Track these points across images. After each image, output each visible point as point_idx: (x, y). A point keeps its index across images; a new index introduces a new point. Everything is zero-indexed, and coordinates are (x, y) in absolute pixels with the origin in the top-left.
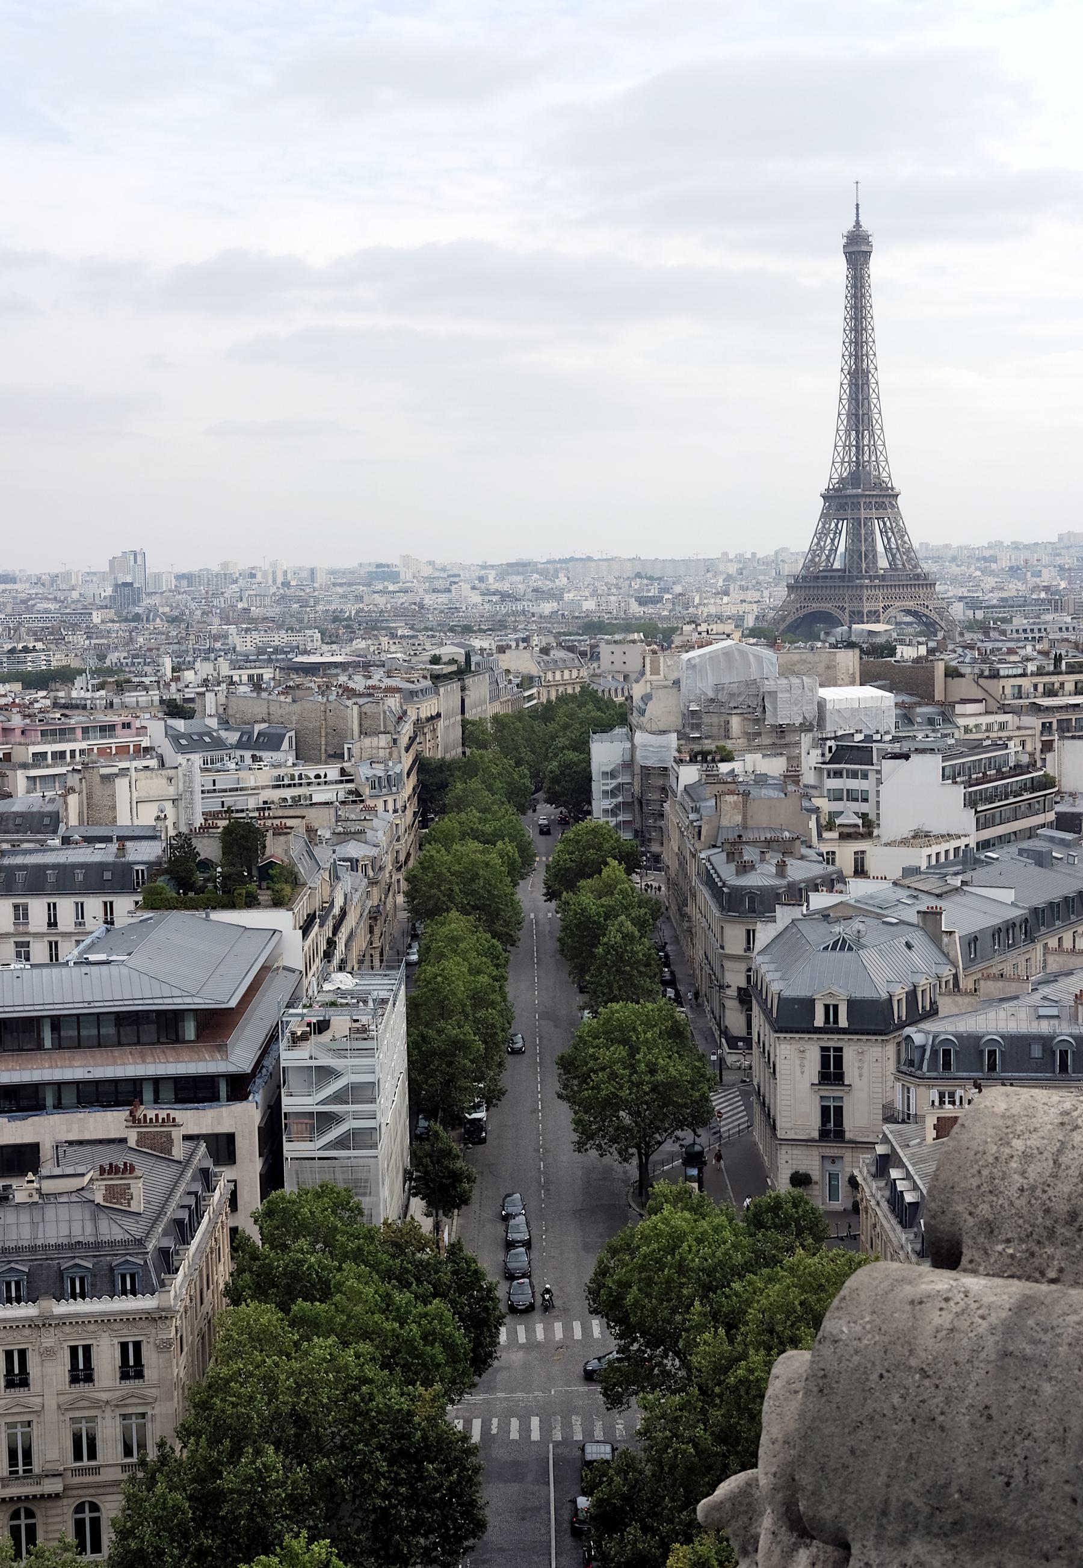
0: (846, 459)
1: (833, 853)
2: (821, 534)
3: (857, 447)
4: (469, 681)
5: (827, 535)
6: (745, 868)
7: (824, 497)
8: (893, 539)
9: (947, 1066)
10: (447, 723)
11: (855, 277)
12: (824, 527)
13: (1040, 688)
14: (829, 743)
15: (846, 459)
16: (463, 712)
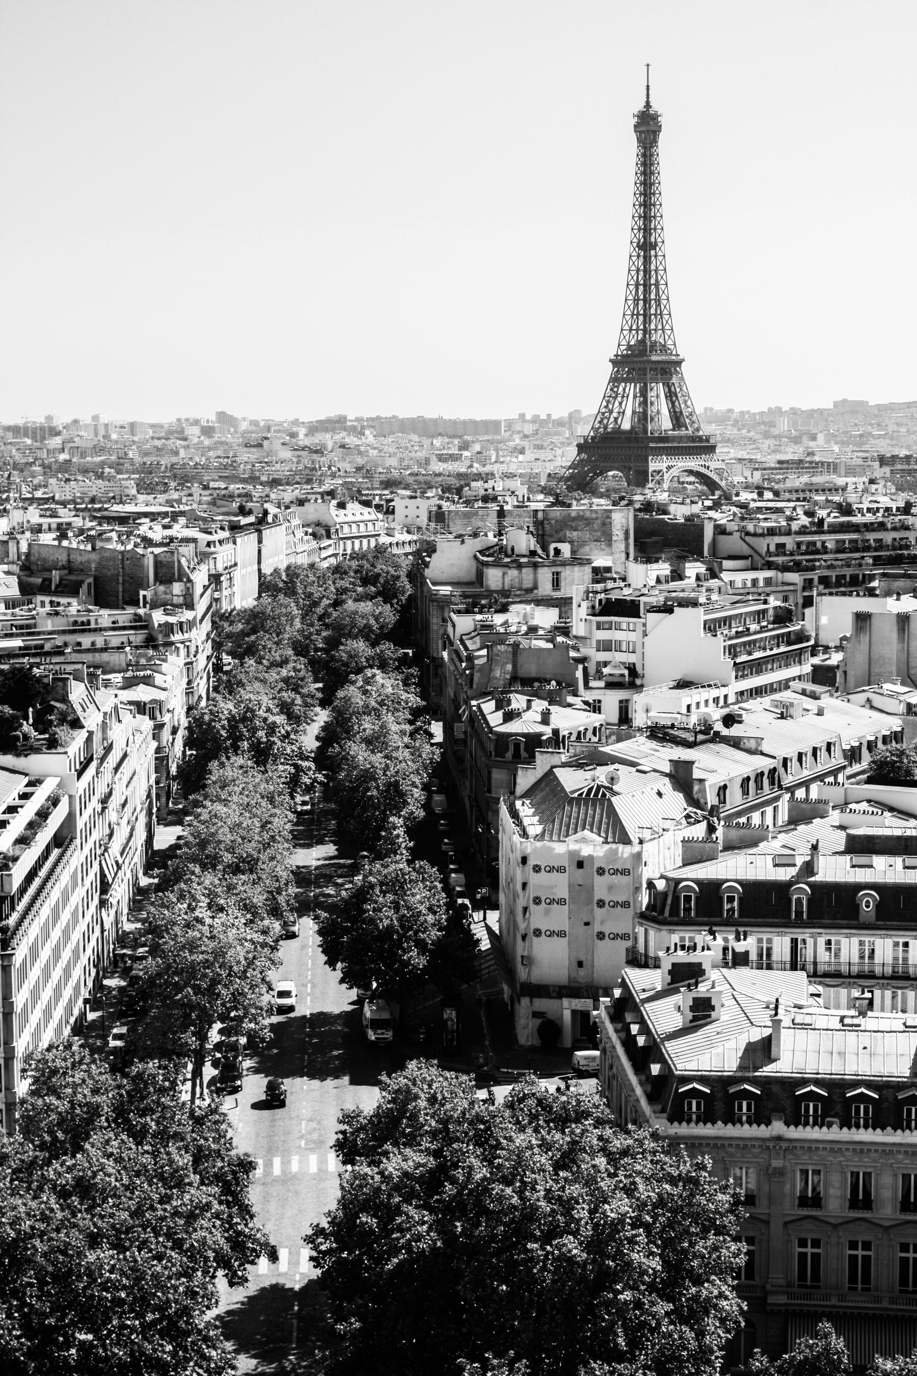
0: (634, 327)
1: (599, 701)
2: (612, 396)
3: (645, 316)
4: (266, 533)
5: (615, 398)
6: (509, 716)
7: (614, 362)
9: (688, 910)
10: (244, 571)
11: (644, 155)
12: (612, 390)
13: (804, 548)
14: (599, 597)
15: (634, 327)
16: (259, 562)
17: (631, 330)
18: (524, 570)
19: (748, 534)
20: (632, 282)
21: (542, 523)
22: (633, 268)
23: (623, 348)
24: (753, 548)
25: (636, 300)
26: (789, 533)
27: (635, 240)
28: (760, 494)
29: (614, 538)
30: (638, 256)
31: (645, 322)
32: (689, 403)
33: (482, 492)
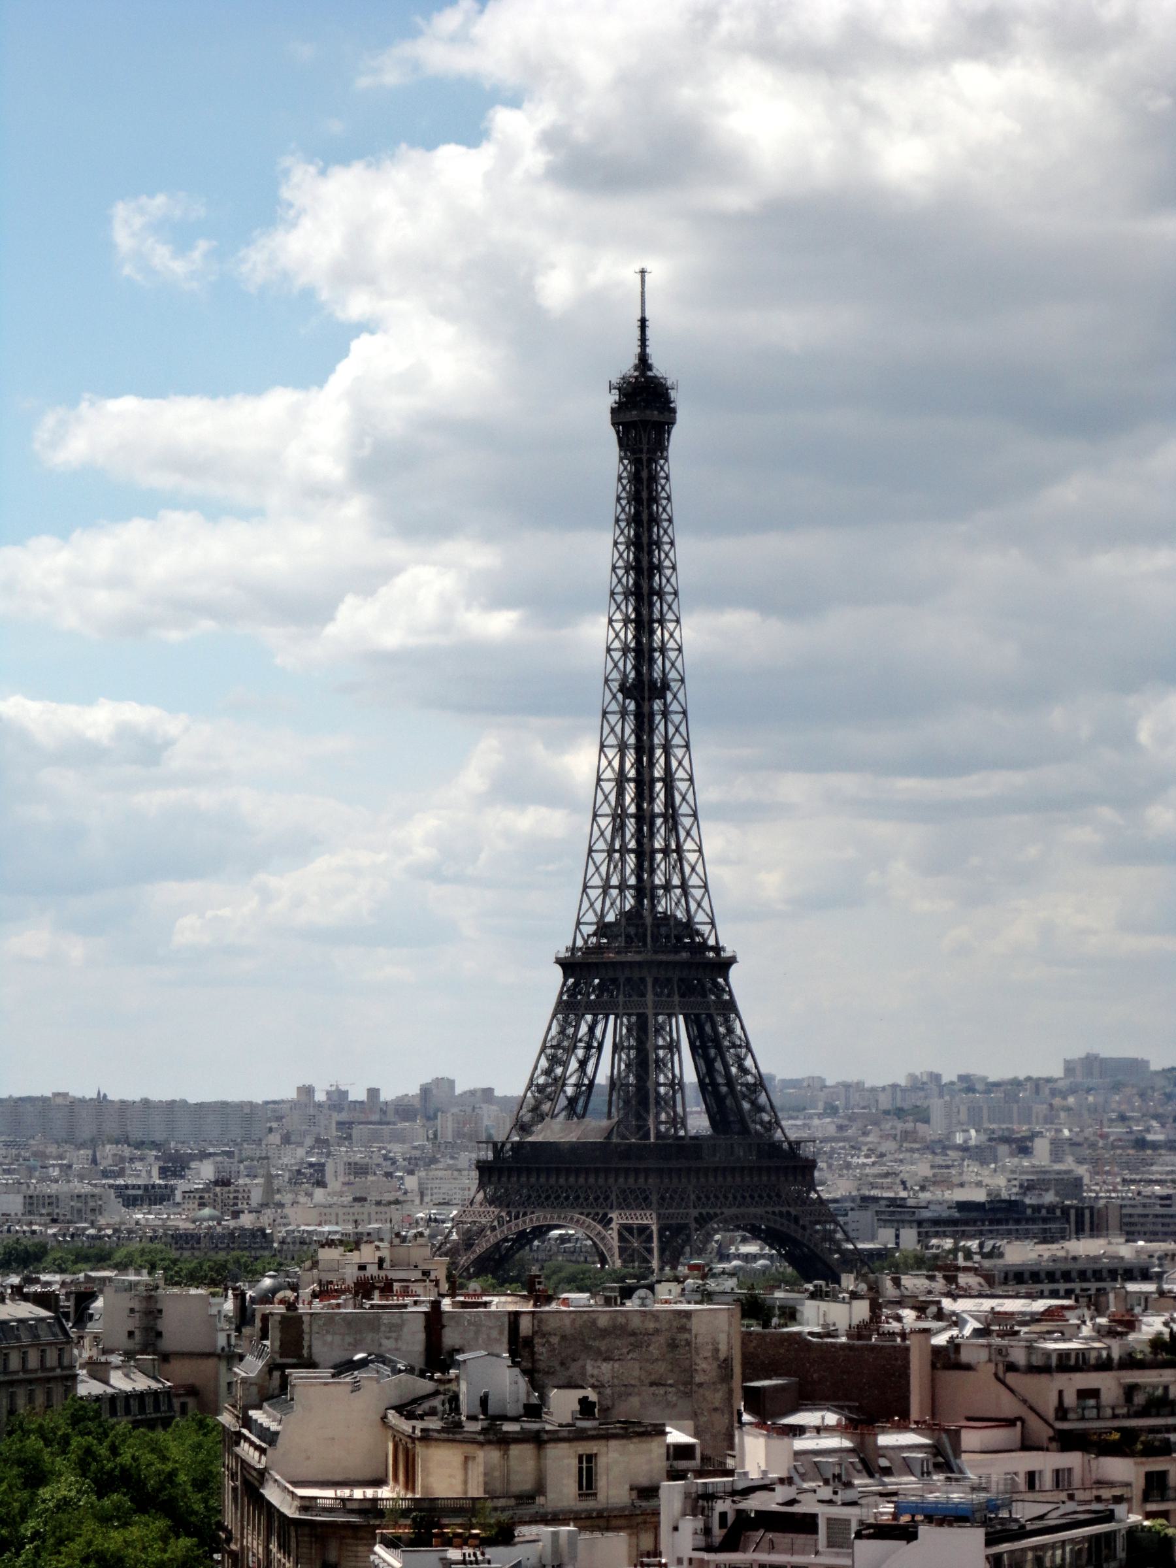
3: (640, 853)
7: (568, 966)
8: (718, 1065)
11: (636, 478)
12: (562, 1032)
14: (721, 1506)
15: (615, 881)
17: (606, 888)
18: (515, 1450)
19: (1011, 1367)
20: (609, 774)
21: (529, 1342)
22: (612, 740)
23: (588, 930)
24: (1024, 1401)
25: (619, 818)
26: (1105, 1365)
27: (615, 675)
28: (951, 1279)
29: (698, 1379)
30: (623, 713)
31: (639, 870)
32: (749, 1063)
33: (351, 1275)
